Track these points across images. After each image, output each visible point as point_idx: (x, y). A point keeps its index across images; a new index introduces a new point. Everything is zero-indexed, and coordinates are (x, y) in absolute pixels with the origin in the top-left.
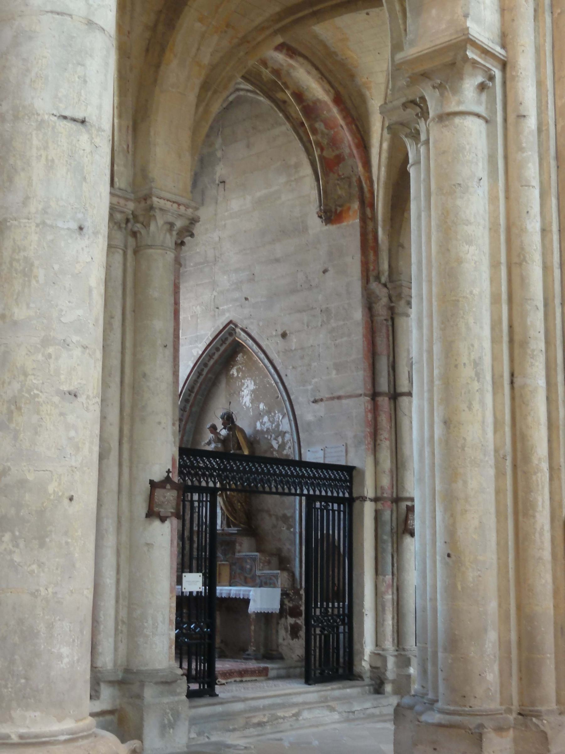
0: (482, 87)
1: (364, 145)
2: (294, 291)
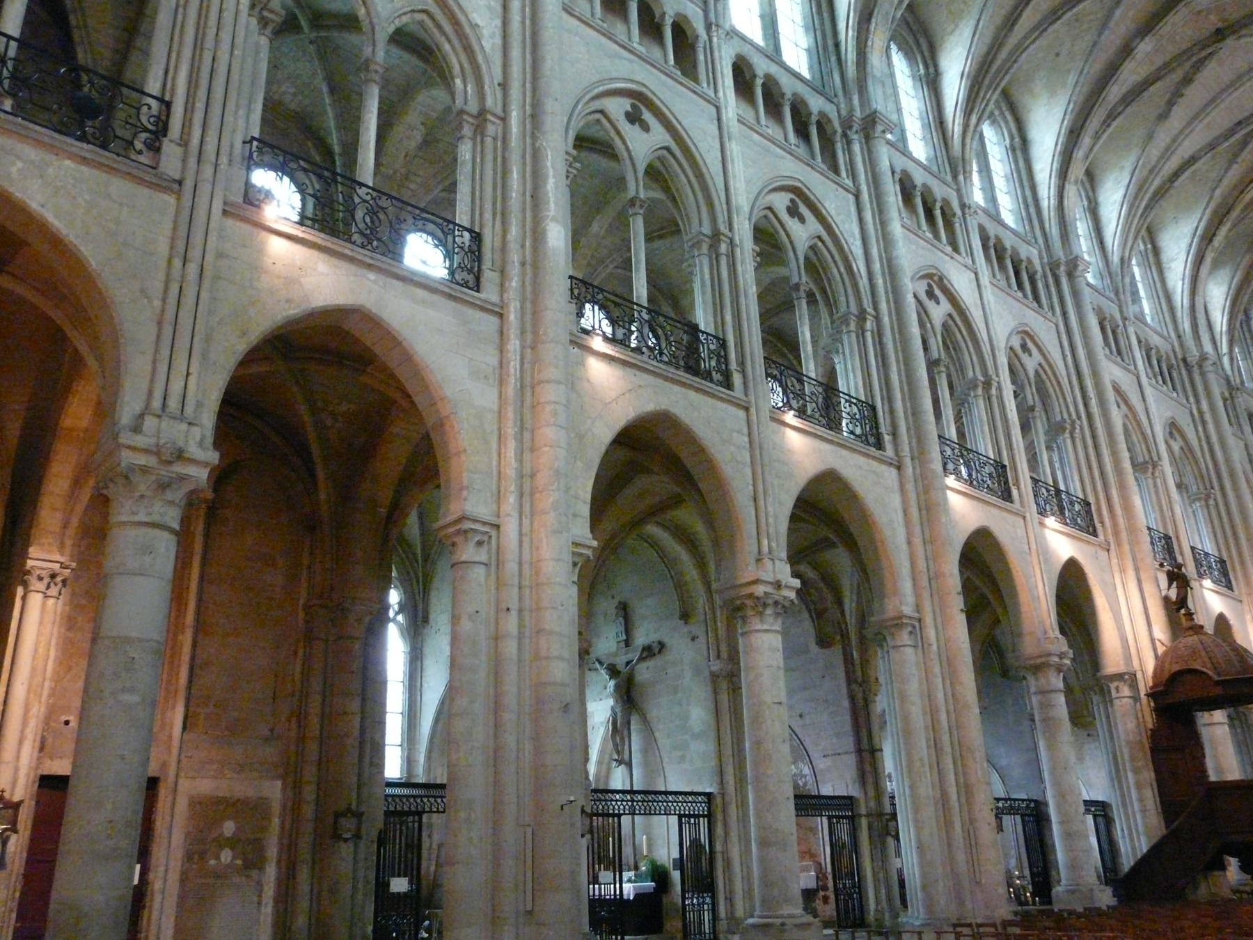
0: (911, 633)
1: (840, 602)
2: (805, 688)
